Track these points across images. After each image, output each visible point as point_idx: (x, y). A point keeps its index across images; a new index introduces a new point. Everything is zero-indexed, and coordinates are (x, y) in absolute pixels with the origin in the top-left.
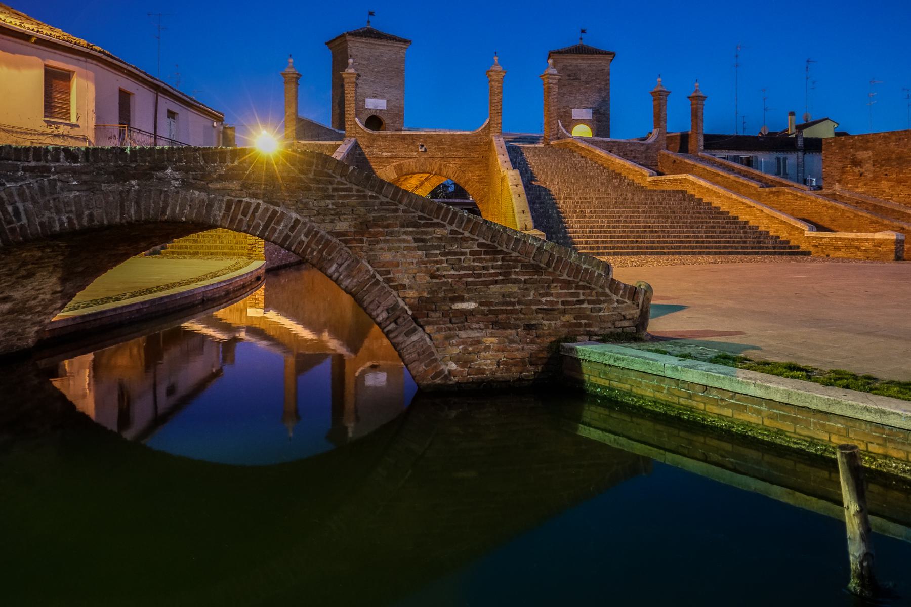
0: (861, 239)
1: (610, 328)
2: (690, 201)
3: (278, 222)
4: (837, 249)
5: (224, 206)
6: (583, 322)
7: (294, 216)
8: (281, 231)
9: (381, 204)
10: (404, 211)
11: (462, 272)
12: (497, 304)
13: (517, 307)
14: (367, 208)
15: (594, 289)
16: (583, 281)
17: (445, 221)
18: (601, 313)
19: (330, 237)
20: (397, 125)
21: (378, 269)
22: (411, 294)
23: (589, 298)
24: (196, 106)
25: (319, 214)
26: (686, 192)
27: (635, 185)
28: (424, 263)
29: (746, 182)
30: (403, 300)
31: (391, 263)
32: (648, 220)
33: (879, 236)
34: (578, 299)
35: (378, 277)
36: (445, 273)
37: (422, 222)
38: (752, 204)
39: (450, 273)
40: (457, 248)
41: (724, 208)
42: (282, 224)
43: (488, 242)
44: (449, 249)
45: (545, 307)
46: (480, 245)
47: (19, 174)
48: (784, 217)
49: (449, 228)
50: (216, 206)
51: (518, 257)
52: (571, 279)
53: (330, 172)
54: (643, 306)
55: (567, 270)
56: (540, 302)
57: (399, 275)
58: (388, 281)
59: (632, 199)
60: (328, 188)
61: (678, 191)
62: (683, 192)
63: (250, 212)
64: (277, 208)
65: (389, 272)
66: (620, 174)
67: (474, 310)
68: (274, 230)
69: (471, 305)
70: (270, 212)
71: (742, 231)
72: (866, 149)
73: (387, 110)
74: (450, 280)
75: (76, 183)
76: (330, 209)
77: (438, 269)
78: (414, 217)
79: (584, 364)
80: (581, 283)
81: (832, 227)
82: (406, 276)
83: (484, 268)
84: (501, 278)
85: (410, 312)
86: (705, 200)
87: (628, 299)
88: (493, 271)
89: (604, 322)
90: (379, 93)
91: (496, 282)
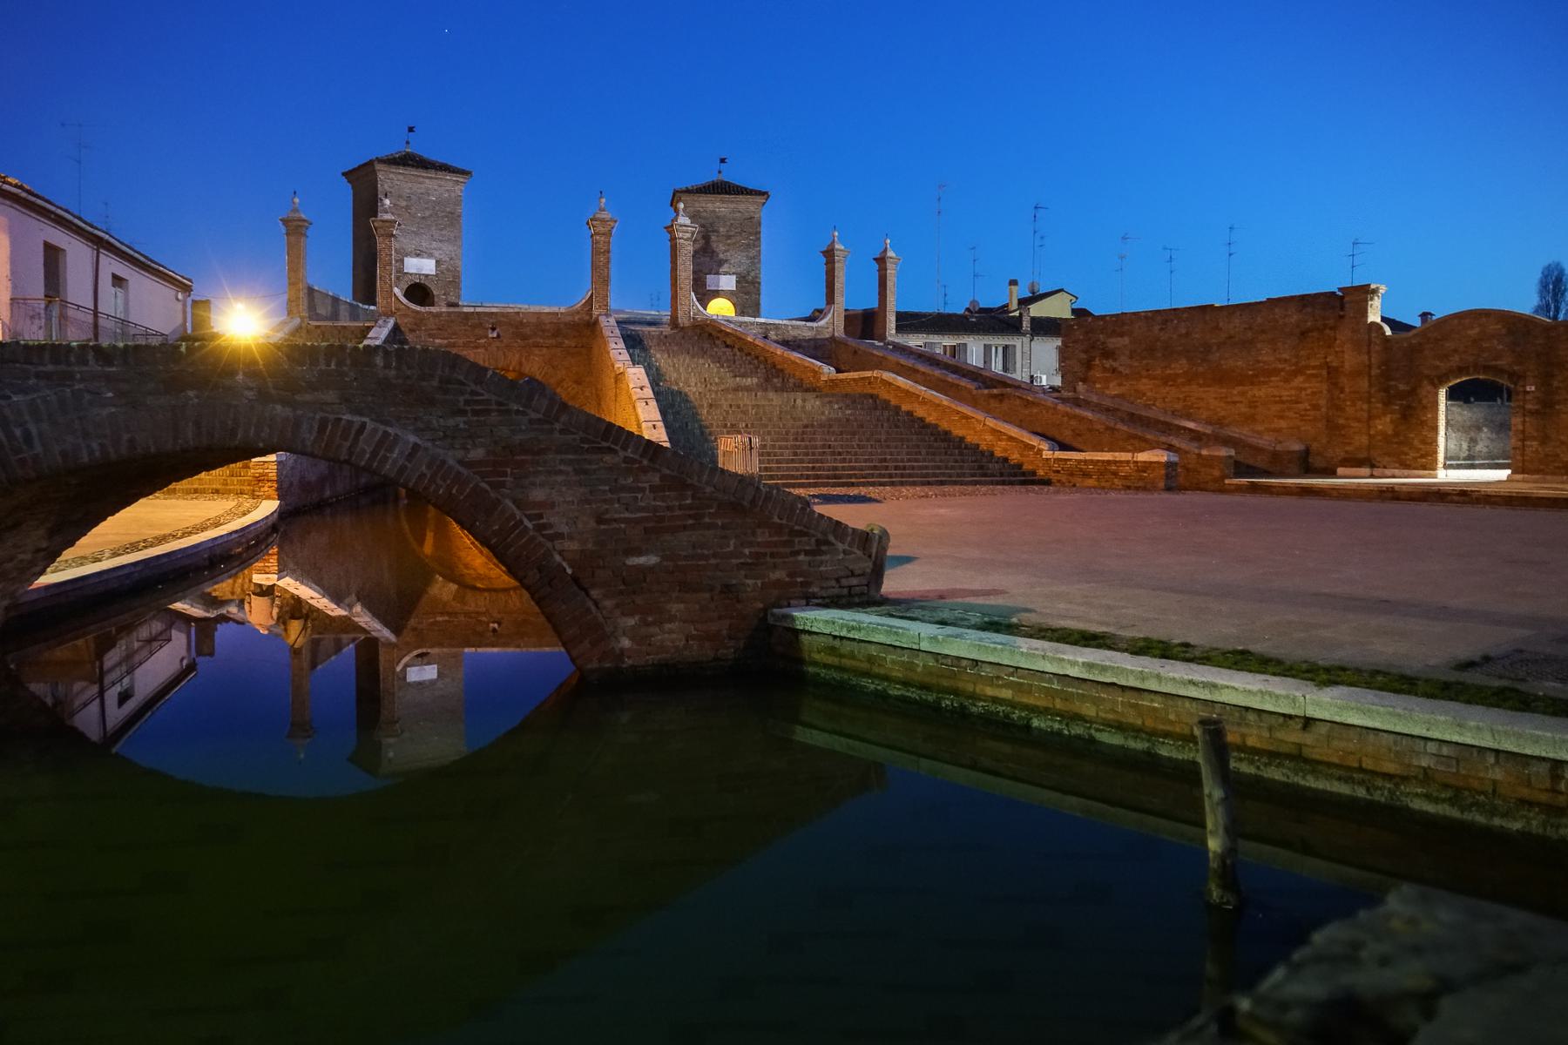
1: (834, 587)
2: (883, 408)
3: (391, 450)
5: (316, 427)
6: (799, 580)
7: (412, 439)
8: (395, 461)
9: (531, 421)
10: (562, 431)
11: (639, 515)
12: (686, 558)
13: (713, 561)
14: (512, 427)
15: (813, 536)
16: (799, 525)
17: (616, 445)
18: (822, 568)
19: (461, 469)
20: (453, 299)
21: (528, 512)
22: (573, 546)
23: (807, 548)
24: (153, 268)
25: (445, 436)
26: (878, 396)
27: (804, 386)
28: (588, 502)
30: (560, 555)
31: (541, 505)
32: (827, 437)
34: (793, 549)
35: (526, 522)
36: (616, 516)
37: (586, 446)
39: (622, 515)
40: (633, 482)
42: (397, 451)
43: (675, 473)
44: (622, 481)
45: (749, 561)
46: (663, 478)
47: (31, 382)
49: (622, 454)
50: (305, 426)
51: (714, 492)
52: (784, 522)
53: (461, 378)
54: (876, 557)
55: (777, 510)
58: (540, 528)
59: (803, 407)
60: (459, 401)
63: (352, 436)
64: (389, 430)
65: (540, 516)
66: (782, 370)
68: (386, 458)
69: (650, 560)
73: (437, 275)
74: (623, 526)
76: (460, 429)
77: (607, 511)
78: (574, 440)
80: (797, 528)
82: (565, 521)
83: (669, 508)
84: (691, 522)
85: (569, 571)
86: (905, 408)
87: (858, 548)
89: (827, 579)
90: (424, 250)
91: (685, 528)
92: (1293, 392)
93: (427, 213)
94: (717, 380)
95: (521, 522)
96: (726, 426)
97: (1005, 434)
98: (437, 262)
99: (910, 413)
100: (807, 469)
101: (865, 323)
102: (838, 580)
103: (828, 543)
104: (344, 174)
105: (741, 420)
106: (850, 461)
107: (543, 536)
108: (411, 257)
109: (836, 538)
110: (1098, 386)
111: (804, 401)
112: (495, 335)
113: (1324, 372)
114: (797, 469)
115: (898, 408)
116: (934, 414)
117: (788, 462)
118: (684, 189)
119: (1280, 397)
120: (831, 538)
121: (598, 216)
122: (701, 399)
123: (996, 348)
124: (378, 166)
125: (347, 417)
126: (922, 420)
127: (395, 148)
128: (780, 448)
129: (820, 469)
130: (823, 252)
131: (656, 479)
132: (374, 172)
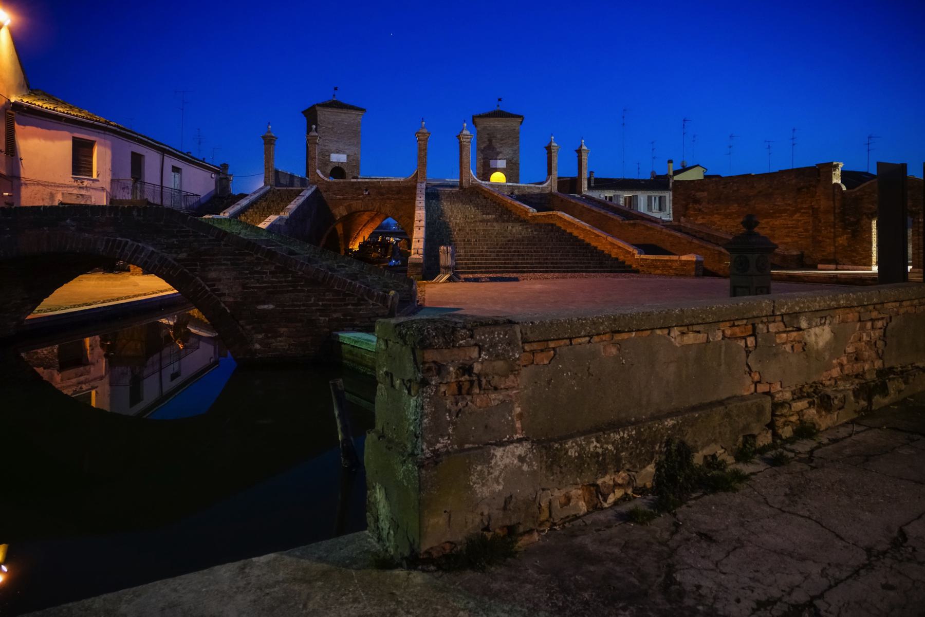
0: (673, 260)
4: (656, 268)
6: (348, 318)
7: (151, 249)
10: (225, 245)
13: (302, 308)
18: (361, 312)
19: (175, 263)
26: (555, 224)
29: (612, 217)
32: (518, 247)
33: (684, 258)
35: (207, 288)
36: (252, 285)
38: (600, 234)
41: (581, 237)
42: (143, 254)
48: (621, 244)
49: (255, 256)
52: (340, 289)
56: (318, 305)
57: (221, 287)
58: (214, 291)
59: (511, 230)
61: (549, 224)
62: (552, 225)
64: (140, 244)
66: (511, 211)
67: (272, 309)
70: (135, 247)
71: (590, 254)
72: (703, 191)
74: (256, 290)
75: (8, 229)
79: (343, 346)
80: (347, 292)
81: (672, 251)
83: (279, 282)
84: (291, 289)
86: (568, 231)
87: (380, 303)
88: (285, 284)
91: (288, 291)
92: (794, 222)
93: (343, 131)
94: (472, 216)
95: (204, 287)
96: (464, 241)
97: (617, 245)
98: (348, 156)
99: (571, 234)
100: (502, 263)
101: (570, 185)
102: (369, 318)
103: (364, 300)
104: (303, 112)
105: (474, 237)
106: (527, 259)
107: (216, 294)
108: (334, 153)
109: (368, 298)
110: (691, 219)
111: (513, 227)
112: (367, 193)
113: (811, 211)
114: (496, 264)
115: (565, 231)
116: (582, 234)
117: (492, 259)
118: (478, 115)
119: (787, 224)
120: (366, 298)
121: (421, 131)
122: (455, 227)
123: (655, 198)
124: (317, 108)
125: (119, 239)
126: (576, 237)
127: (328, 97)
128: (491, 252)
129: (508, 263)
130: (545, 147)
131: (273, 268)
132: (316, 111)
